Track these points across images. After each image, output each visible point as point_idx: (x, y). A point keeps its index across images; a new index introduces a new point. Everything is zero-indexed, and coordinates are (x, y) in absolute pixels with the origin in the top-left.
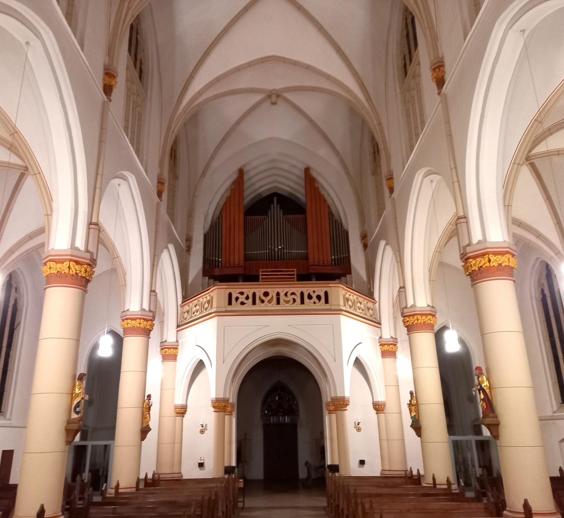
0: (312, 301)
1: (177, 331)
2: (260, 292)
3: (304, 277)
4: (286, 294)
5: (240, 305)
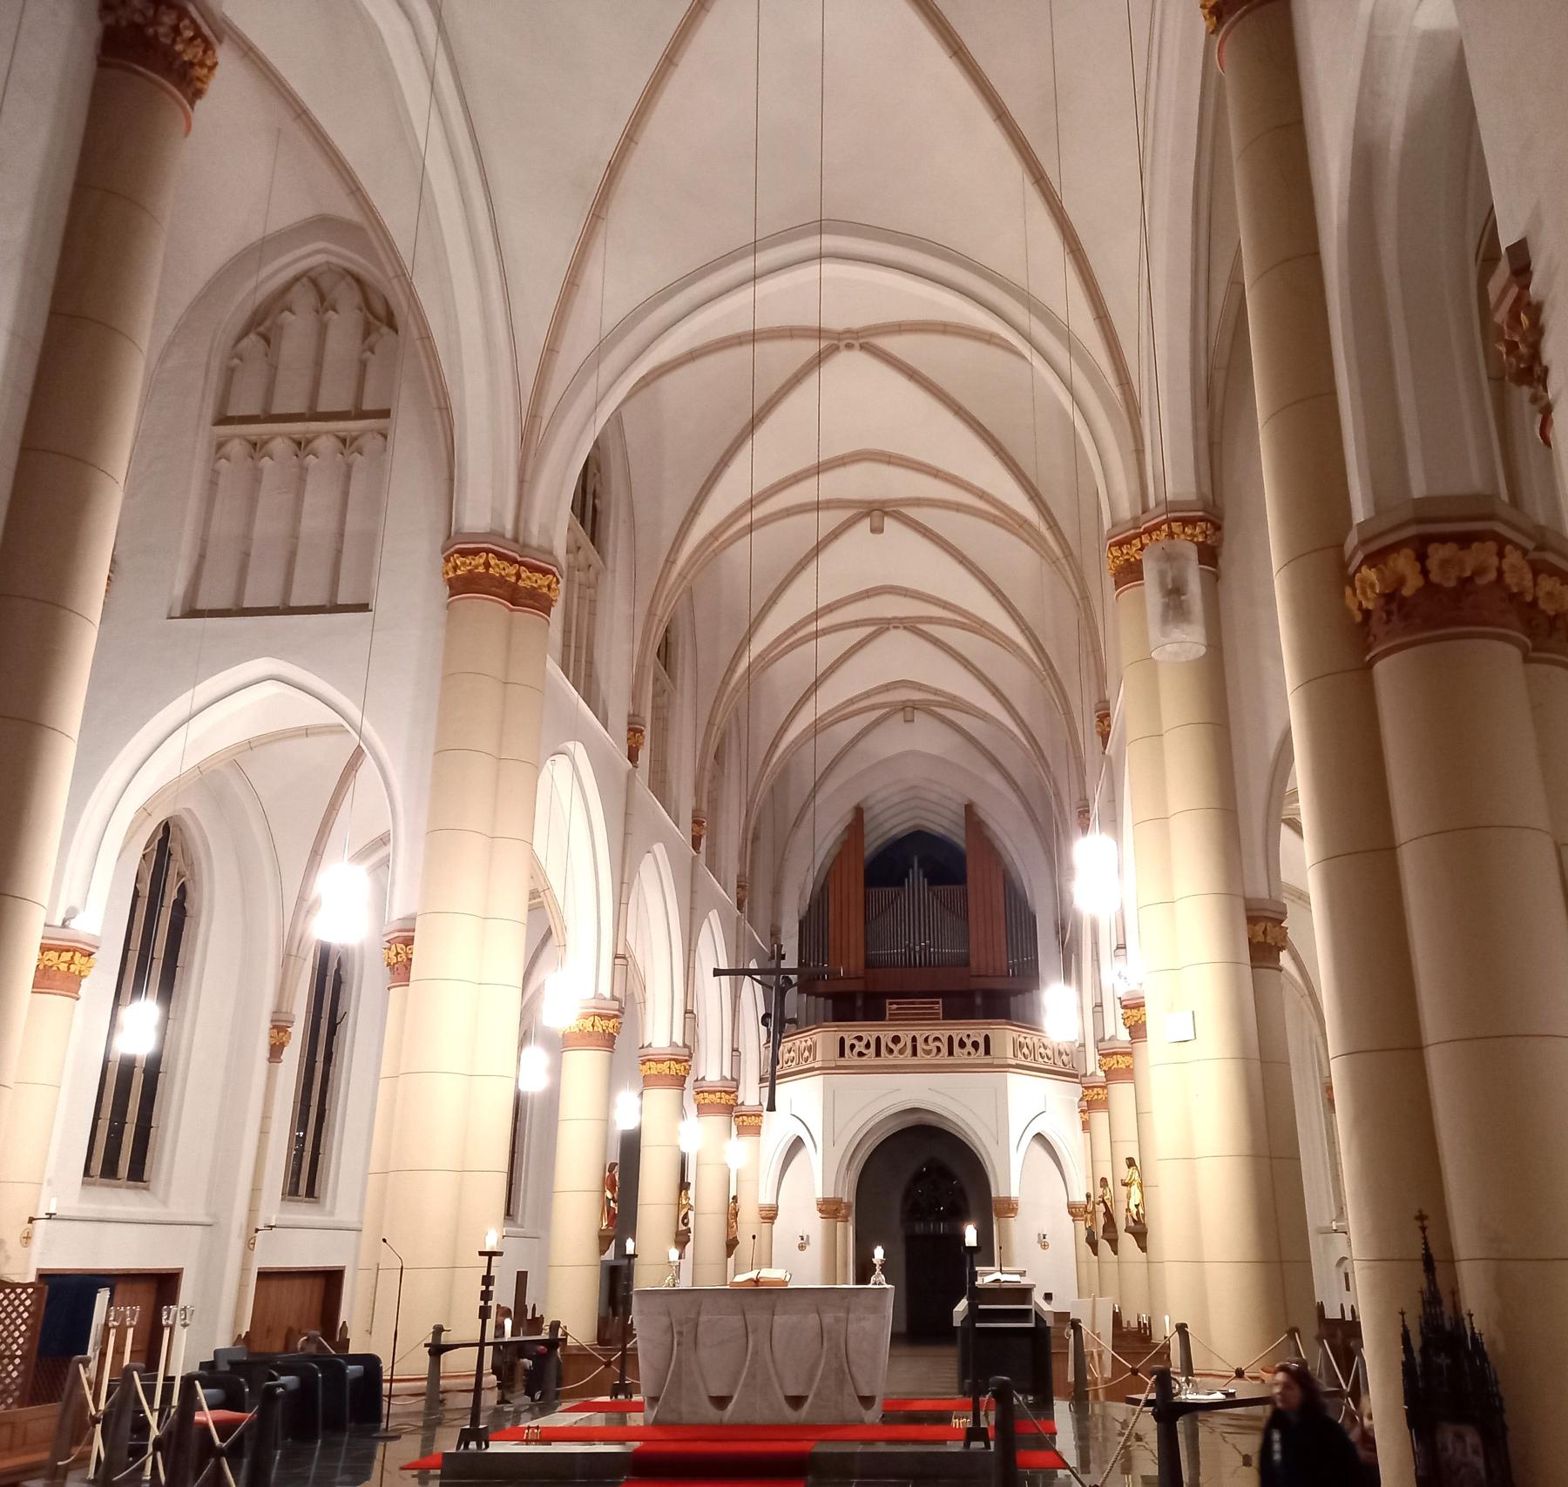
2: (886, 1037)
3: (951, 1014)
4: (926, 1040)
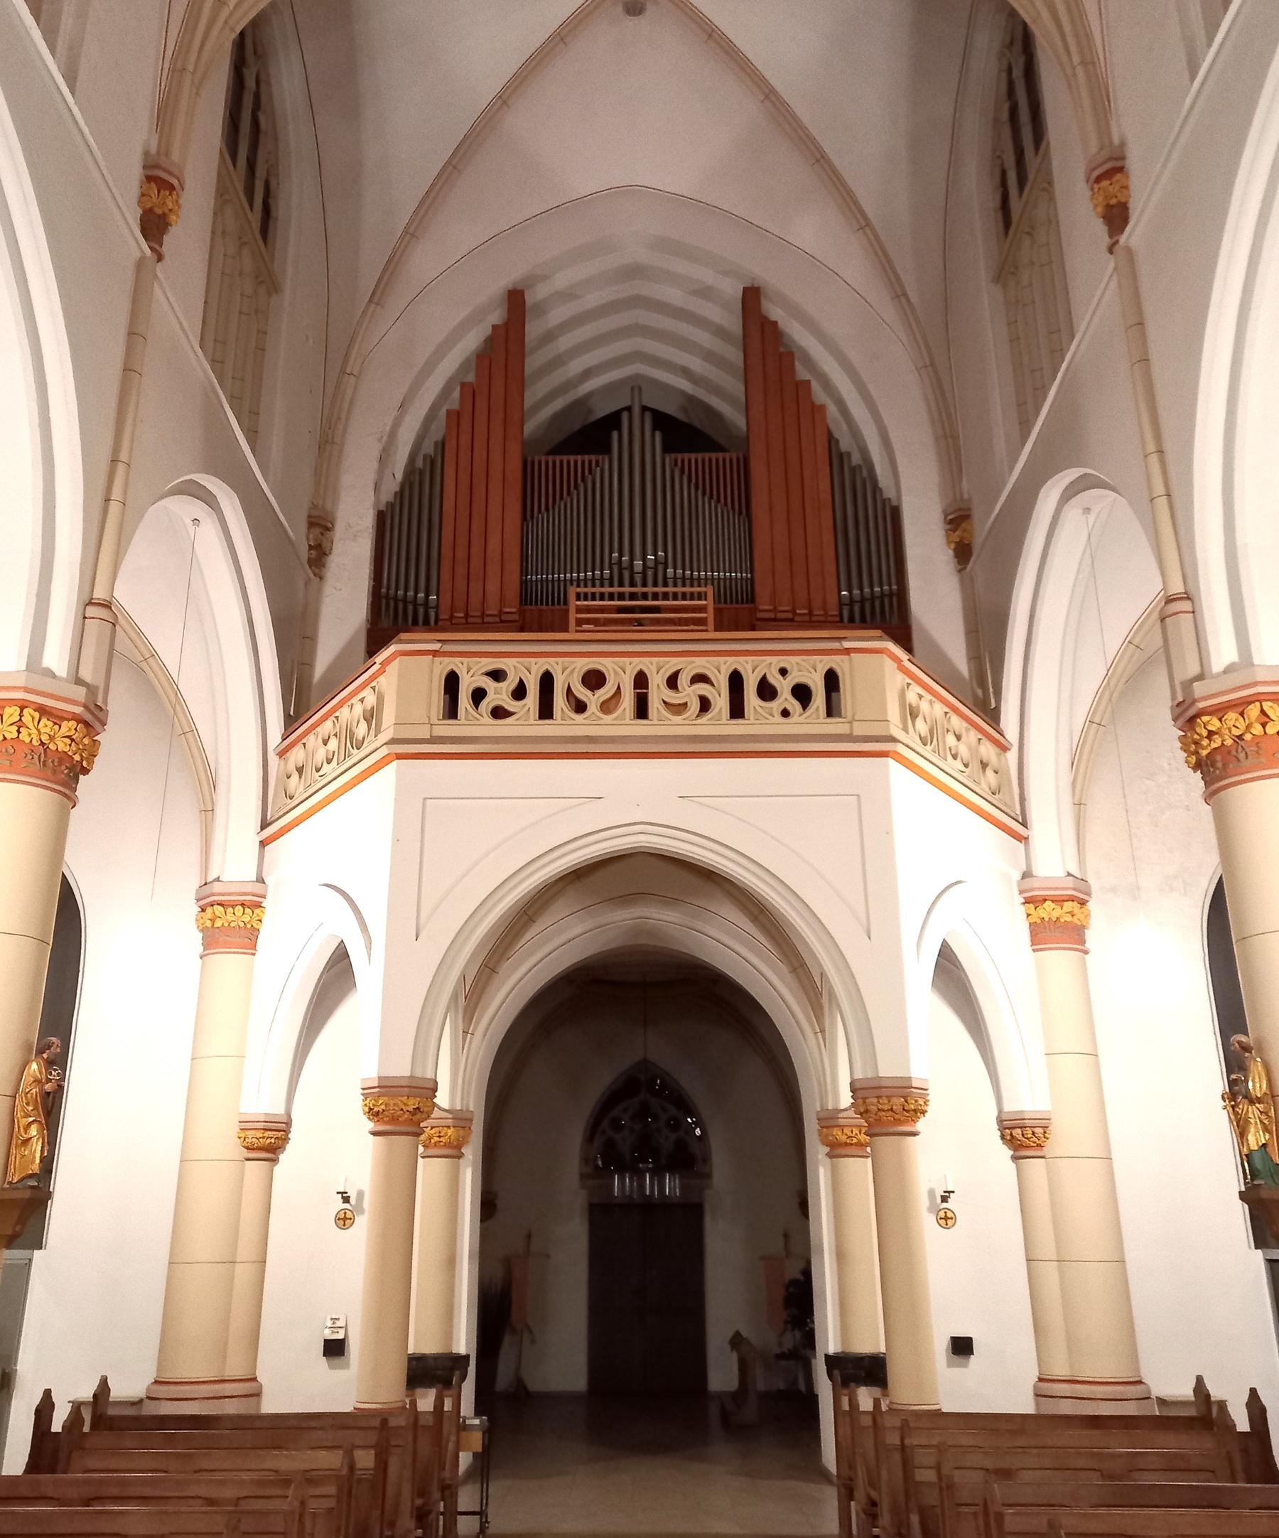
0: (776, 705)
2: (568, 673)
4: (672, 682)
5: (488, 719)
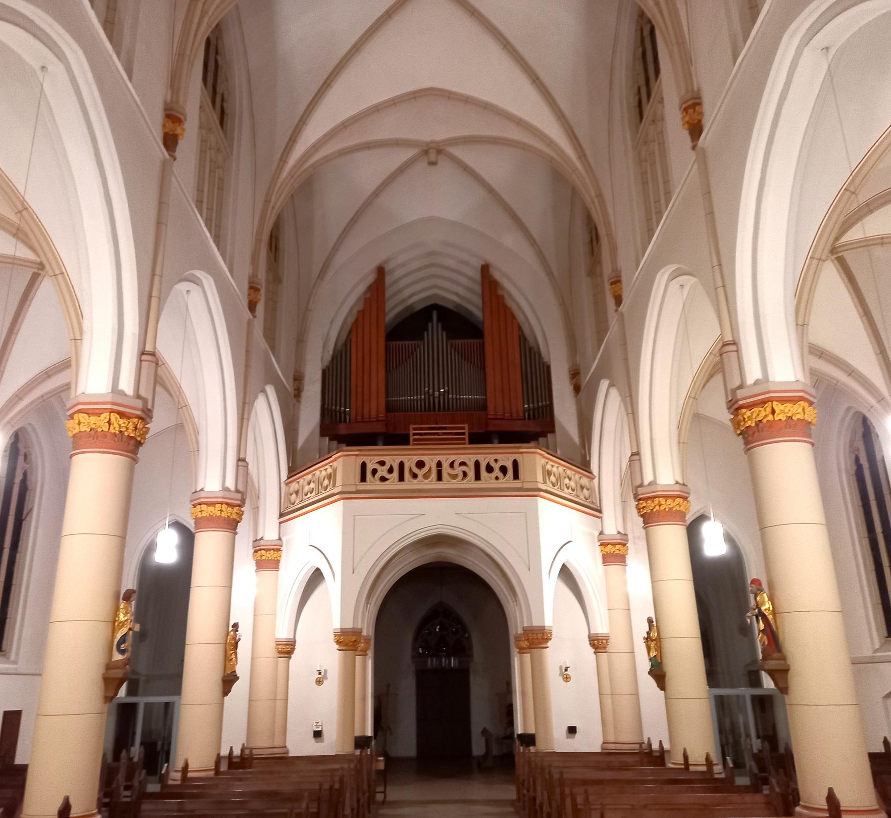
0: (493, 475)
1: (280, 523)
2: (410, 462)
3: (480, 438)
4: (452, 465)
5: (378, 482)
